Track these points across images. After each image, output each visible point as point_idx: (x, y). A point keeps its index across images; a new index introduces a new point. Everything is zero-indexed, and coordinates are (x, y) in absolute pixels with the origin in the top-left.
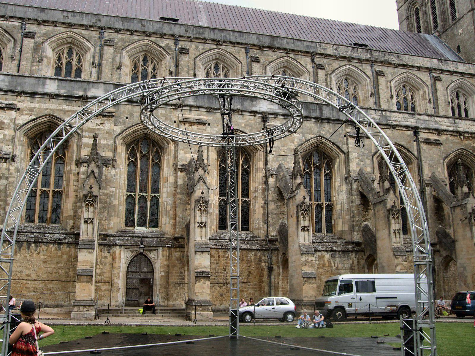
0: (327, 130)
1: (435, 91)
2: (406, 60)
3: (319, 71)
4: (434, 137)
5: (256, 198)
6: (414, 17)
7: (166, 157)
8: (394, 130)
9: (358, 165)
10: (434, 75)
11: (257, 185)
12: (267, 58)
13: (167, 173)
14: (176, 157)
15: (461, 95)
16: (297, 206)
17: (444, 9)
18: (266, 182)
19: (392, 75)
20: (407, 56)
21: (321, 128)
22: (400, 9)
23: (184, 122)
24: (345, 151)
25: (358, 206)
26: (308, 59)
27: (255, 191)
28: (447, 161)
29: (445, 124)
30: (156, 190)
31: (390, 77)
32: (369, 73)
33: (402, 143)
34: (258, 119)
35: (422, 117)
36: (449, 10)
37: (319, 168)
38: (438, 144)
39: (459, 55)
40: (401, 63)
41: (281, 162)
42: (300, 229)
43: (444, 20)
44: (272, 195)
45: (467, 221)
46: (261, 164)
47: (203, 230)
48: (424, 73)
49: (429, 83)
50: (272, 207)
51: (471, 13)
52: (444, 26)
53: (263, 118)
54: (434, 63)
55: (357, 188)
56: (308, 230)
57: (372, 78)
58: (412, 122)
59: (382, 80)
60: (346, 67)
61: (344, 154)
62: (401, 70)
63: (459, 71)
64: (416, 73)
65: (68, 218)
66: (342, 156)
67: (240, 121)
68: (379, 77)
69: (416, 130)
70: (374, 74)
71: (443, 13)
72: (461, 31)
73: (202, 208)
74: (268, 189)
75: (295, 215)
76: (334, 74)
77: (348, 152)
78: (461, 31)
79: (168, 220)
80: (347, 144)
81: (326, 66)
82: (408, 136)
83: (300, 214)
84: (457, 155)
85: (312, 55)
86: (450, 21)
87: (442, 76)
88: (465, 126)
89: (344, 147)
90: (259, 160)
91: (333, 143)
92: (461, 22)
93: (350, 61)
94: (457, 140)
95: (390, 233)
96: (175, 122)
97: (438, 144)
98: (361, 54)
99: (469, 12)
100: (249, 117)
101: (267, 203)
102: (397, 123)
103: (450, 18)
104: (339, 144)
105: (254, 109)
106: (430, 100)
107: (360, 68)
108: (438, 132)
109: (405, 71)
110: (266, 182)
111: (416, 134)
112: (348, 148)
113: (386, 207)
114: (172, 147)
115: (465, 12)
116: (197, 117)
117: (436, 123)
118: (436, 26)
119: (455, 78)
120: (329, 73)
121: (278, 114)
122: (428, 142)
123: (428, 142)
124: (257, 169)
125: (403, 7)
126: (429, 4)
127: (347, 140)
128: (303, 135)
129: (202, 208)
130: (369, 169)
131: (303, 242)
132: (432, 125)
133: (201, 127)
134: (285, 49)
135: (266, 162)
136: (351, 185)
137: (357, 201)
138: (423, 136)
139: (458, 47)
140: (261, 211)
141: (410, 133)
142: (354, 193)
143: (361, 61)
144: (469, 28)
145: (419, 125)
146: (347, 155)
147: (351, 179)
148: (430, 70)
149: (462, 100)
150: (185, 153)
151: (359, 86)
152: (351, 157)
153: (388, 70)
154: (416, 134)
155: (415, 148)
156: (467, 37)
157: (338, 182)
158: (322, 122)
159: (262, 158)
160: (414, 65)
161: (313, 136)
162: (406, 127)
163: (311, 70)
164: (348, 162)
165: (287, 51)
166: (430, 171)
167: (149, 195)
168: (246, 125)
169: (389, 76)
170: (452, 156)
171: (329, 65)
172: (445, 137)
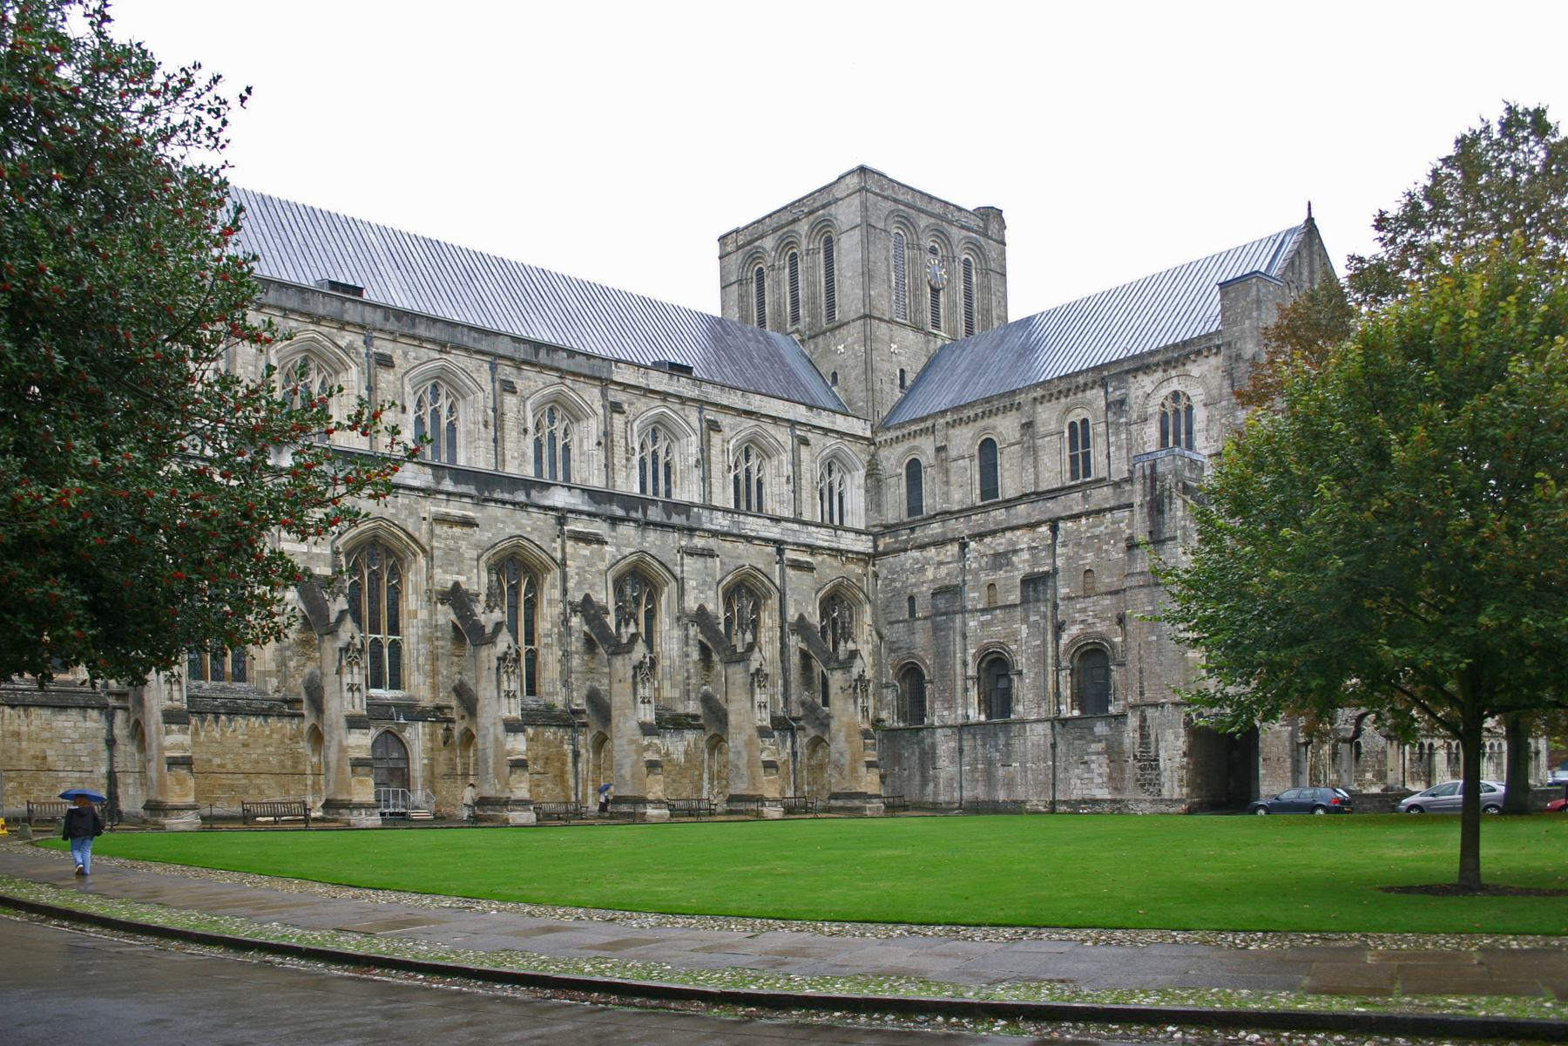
0: (653, 538)
1: (796, 463)
2: (757, 403)
3: (616, 416)
4: (805, 558)
5: (547, 646)
6: (754, 285)
7: (411, 576)
8: (749, 545)
9: (696, 598)
10: (798, 432)
11: (549, 626)
12: (527, 383)
13: (412, 602)
14: (430, 578)
15: (834, 468)
16: (635, 668)
17: (814, 294)
18: (565, 621)
19: (731, 429)
20: (758, 397)
21: (643, 538)
22: (726, 259)
23: (442, 520)
24: (679, 576)
25: (695, 662)
26: (596, 392)
27: (547, 635)
28: (820, 595)
29: (821, 537)
30: (394, 628)
31: (727, 432)
32: (696, 424)
33: (759, 566)
34: (551, 518)
35: (790, 525)
36: (823, 298)
37: (637, 601)
38: (809, 568)
39: (834, 389)
40: (749, 408)
41: (587, 591)
42: (639, 700)
43: (814, 315)
44: (576, 644)
45: (851, 690)
46: (557, 594)
47: (512, 700)
48: (783, 429)
49: (789, 447)
50: (576, 661)
51: (862, 321)
52: (811, 326)
53: (559, 518)
54: (800, 413)
55: (696, 636)
56: (649, 702)
57: (699, 433)
58: (774, 532)
59: (716, 439)
60: (657, 408)
61: (677, 580)
62: (748, 424)
63: (836, 428)
64: (771, 428)
65: (265, 674)
66: (673, 584)
67: (524, 521)
68: (712, 433)
69: (779, 545)
70: (704, 425)
71: (813, 298)
72: (841, 348)
73: (510, 670)
74: (570, 635)
75: (630, 680)
76: (638, 422)
77: (683, 579)
78: (841, 348)
79: (421, 679)
80: (682, 565)
81: (626, 407)
82: (768, 554)
83: (639, 679)
84: (835, 586)
85: (605, 383)
86: (824, 320)
87: (809, 436)
88: (849, 542)
89: (677, 570)
90: (553, 586)
91: (660, 562)
92: (844, 331)
93: (665, 400)
94: (836, 563)
95: (753, 706)
96: (424, 519)
97: (809, 568)
98: (682, 386)
99: (859, 318)
100: (536, 514)
101: (567, 655)
102: (753, 534)
103: (824, 313)
104: (670, 566)
105: (547, 503)
106: (788, 478)
107: (681, 413)
108: (812, 549)
109: (753, 423)
110: (565, 621)
111: (780, 552)
112: (682, 572)
113: (748, 671)
114: (422, 560)
115: (853, 316)
116: (459, 513)
117: (810, 535)
118: (796, 319)
119: (831, 442)
120: (631, 418)
121: (581, 513)
122: (797, 565)
123: (797, 565)
124: (550, 602)
125: (733, 257)
126: (787, 270)
127: (682, 558)
128: (616, 545)
129: (510, 670)
130: (710, 607)
131: (643, 719)
132: (803, 539)
133: (466, 530)
134: (557, 369)
135: (565, 591)
136: (686, 629)
137: (695, 655)
138: (790, 554)
139: (834, 375)
140: (558, 667)
141: (771, 549)
142: (691, 642)
143: (683, 400)
144: (856, 347)
145: (785, 538)
146: (681, 583)
147: (685, 620)
148: (793, 424)
149: (836, 477)
150: (445, 572)
151: (676, 444)
152: (686, 587)
153: (725, 420)
154: (780, 552)
155: (777, 573)
156: (851, 362)
157: (664, 623)
158: (644, 529)
159: (558, 583)
161: (633, 550)
162: (767, 540)
163: (601, 411)
164: (683, 594)
165: (563, 373)
166: (796, 610)
167: (385, 638)
168: (534, 529)
169: (727, 430)
170: (828, 587)
171: (631, 404)
172: (820, 558)
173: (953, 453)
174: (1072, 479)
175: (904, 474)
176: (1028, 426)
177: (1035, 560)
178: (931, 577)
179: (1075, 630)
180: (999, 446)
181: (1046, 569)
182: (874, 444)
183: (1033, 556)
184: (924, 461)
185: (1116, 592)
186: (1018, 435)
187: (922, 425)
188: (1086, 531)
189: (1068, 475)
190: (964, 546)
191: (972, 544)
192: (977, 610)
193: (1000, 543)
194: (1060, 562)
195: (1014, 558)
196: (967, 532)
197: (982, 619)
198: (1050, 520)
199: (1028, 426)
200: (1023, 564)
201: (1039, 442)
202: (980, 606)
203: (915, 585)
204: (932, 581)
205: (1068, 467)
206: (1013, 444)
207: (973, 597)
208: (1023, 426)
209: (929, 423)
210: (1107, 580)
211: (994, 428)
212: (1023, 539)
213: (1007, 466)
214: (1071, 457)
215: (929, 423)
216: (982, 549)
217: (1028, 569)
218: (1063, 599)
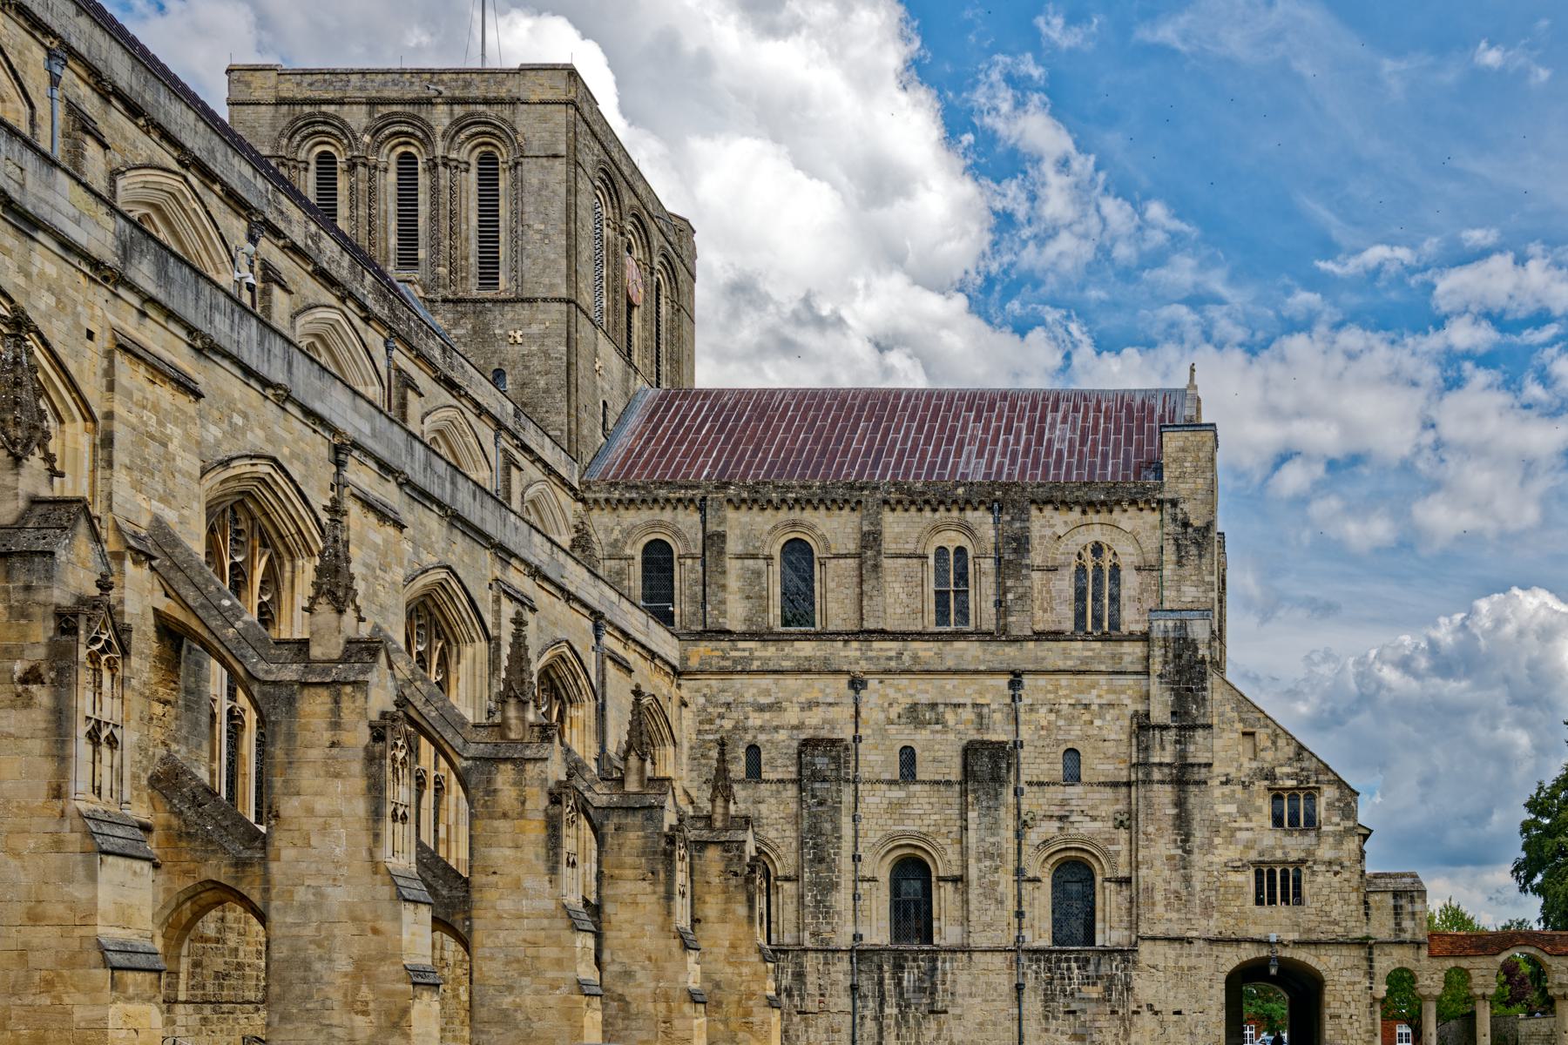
160: (475, 396)
173: (733, 545)
174: (938, 624)
175: (639, 558)
176: (871, 540)
177: (981, 721)
178: (795, 722)
179: (1052, 827)
180: (816, 554)
181: (1003, 738)
182: (583, 500)
183: (980, 716)
184: (678, 549)
185: (1115, 785)
186: (852, 547)
187: (681, 493)
188: (1066, 696)
189: (933, 617)
190: (857, 684)
191: (873, 683)
192: (879, 781)
193: (923, 690)
194: (1025, 733)
195: (950, 717)
196: (864, 665)
197: (888, 794)
198: (1012, 673)
199: (871, 540)
200: (961, 727)
201: (887, 563)
202: (887, 776)
203: (762, 729)
204: (795, 728)
205: (932, 606)
206: (845, 556)
207: (876, 759)
208: (864, 535)
209: (699, 493)
210: (1100, 767)
211: (812, 528)
212: (964, 690)
213: (831, 585)
214: (937, 593)
215: (699, 493)
216: (891, 693)
217: (973, 735)
218: (1030, 784)
